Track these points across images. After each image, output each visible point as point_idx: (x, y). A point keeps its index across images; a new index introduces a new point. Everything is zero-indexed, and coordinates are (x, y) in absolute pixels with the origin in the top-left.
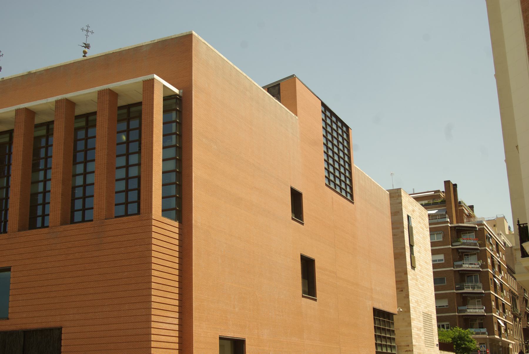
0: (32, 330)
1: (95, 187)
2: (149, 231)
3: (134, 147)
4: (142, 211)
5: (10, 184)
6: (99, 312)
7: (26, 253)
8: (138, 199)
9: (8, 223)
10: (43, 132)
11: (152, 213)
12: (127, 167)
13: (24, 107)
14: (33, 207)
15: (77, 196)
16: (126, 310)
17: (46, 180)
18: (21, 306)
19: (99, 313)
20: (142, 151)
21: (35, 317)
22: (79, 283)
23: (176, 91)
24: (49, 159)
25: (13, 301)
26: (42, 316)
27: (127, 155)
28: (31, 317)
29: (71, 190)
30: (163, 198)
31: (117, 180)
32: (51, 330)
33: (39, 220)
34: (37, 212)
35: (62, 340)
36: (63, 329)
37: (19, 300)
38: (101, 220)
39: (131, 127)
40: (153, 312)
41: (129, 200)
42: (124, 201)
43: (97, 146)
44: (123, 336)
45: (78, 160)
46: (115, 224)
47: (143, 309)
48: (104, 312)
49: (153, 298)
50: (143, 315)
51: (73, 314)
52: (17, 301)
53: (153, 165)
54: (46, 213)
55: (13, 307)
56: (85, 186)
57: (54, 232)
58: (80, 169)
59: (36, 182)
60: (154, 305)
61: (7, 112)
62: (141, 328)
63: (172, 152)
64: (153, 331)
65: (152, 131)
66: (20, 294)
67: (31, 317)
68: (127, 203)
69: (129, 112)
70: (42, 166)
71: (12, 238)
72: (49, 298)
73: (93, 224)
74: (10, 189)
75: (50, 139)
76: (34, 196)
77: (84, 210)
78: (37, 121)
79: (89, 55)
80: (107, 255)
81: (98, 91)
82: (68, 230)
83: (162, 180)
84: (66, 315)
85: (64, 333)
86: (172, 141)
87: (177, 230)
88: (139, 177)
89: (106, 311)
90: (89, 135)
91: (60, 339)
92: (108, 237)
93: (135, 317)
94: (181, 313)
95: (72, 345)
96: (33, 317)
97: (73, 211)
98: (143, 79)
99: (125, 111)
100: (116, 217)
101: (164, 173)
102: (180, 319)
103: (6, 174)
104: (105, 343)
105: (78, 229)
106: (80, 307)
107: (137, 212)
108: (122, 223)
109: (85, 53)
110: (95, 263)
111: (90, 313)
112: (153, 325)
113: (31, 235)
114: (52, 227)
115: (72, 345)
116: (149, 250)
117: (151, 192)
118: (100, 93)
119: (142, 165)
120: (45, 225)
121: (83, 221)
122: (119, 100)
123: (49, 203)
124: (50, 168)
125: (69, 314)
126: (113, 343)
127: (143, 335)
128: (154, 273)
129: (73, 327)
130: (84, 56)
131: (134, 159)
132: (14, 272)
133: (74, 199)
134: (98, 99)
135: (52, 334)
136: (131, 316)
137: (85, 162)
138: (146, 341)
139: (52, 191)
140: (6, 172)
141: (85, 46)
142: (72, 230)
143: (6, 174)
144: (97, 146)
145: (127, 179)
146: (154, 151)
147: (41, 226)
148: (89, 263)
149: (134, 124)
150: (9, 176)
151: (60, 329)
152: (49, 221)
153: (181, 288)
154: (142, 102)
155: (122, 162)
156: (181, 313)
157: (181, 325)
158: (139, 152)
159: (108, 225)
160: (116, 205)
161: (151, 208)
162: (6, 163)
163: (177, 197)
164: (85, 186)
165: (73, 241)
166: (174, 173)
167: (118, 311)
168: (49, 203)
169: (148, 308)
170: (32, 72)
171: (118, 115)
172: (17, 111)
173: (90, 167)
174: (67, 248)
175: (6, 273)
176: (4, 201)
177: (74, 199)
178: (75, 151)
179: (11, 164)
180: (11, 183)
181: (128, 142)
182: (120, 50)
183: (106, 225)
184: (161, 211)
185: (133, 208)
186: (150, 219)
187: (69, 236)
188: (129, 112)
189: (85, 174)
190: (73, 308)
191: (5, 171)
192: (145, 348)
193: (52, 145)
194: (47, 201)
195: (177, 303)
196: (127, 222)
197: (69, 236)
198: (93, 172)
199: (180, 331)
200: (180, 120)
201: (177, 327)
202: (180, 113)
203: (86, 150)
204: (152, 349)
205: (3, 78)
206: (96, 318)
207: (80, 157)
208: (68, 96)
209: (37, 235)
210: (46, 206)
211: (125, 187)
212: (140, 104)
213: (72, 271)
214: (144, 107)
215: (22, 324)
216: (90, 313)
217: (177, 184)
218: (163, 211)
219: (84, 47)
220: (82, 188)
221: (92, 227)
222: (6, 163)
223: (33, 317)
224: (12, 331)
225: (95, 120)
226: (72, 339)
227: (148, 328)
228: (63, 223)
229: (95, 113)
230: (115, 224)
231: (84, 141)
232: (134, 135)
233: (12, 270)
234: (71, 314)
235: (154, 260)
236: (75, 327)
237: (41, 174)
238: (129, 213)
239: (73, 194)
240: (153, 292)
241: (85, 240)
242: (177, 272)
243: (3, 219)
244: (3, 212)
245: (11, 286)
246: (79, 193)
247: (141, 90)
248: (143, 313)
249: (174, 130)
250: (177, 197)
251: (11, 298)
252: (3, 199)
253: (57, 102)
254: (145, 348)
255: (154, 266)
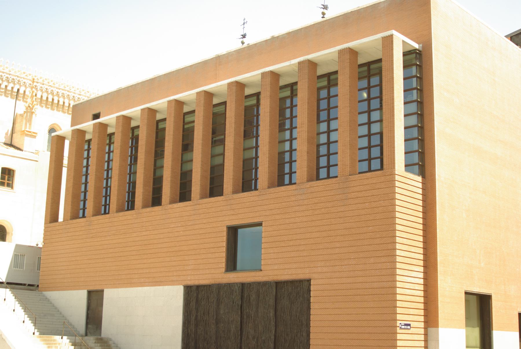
0: (283, 281)
1: (339, 144)
2: (392, 186)
3: (375, 104)
4: (385, 167)
5: (259, 144)
6: (346, 265)
7: (276, 209)
8: (381, 155)
9: (258, 181)
10: (287, 93)
11: (395, 169)
12: (369, 123)
13: (269, 70)
14: (281, 165)
15: (321, 154)
16: (371, 263)
17: (292, 139)
18: (272, 259)
19: (345, 266)
20: (384, 107)
21: (286, 269)
22: (326, 237)
23: (416, 46)
24: (294, 119)
25: (265, 254)
26: (292, 269)
27: (369, 112)
28: (282, 269)
29: (315, 148)
30: (406, 153)
31: (360, 137)
32: (301, 281)
33: (287, 177)
34: (284, 170)
35: (311, 291)
36: (312, 281)
37: (271, 253)
38: (345, 176)
39: (372, 84)
40: (398, 265)
41: (372, 157)
42: (367, 157)
43: (339, 104)
44: (369, 289)
45: (321, 119)
46: (359, 180)
47: (388, 262)
48: (350, 265)
49: (398, 252)
50: (389, 269)
51: (321, 267)
52: (269, 253)
53: (394, 121)
54: (293, 171)
55: (265, 259)
56: (329, 143)
57: (301, 189)
58: (323, 127)
59: (283, 141)
60: (398, 259)
61: (254, 76)
62: (386, 281)
63: (413, 107)
64: (398, 284)
65: (393, 87)
66: (271, 248)
67: (282, 269)
68: (370, 159)
69: (369, 70)
70: (288, 126)
71: (263, 195)
72: (298, 251)
73: (337, 180)
74: (259, 149)
75: (294, 99)
76: (281, 154)
77: (328, 167)
78: (282, 82)
79: (327, 17)
80: (352, 210)
81: (339, 51)
82: (314, 187)
83: (405, 136)
84: (315, 267)
85: (313, 285)
86: (413, 96)
87: (420, 185)
88: (381, 134)
89: (352, 265)
90: (331, 94)
91: (309, 291)
92: (352, 193)
93: (381, 270)
94: (426, 267)
95: (321, 296)
96: (284, 269)
97: (318, 168)
98: (382, 36)
99: (365, 68)
100: (360, 173)
101: (405, 128)
102: (425, 273)
103: (255, 135)
104: (352, 295)
105: (324, 185)
106: (328, 260)
107: (379, 168)
108: (366, 179)
109: (323, 14)
110: (341, 218)
111: (337, 266)
112: (398, 278)
113: (279, 192)
114: (299, 183)
115: (321, 296)
116: (393, 204)
117: (394, 147)
118: (341, 52)
119: (384, 122)
120: (293, 182)
121: (328, 177)
122: (359, 58)
123: (295, 161)
124: (296, 128)
125: (317, 267)
126: (359, 295)
127: (388, 288)
128: (398, 227)
129: (321, 279)
130: (323, 17)
131: (375, 116)
132: (265, 226)
133: (318, 157)
134: (339, 58)
135: (301, 286)
136: (376, 269)
137: (329, 120)
138: (391, 294)
139: (298, 149)
140: (255, 132)
141: (323, 7)
142: (318, 186)
143: (255, 135)
144: (339, 105)
145: (369, 135)
146: (395, 107)
147: (288, 183)
148: (334, 218)
149: (375, 81)
150: (257, 136)
151: (309, 281)
152: (296, 178)
153: (426, 243)
154: (382, 59)
155: (364, 118)
156: (426, 267)
157: (426, 279)
158: (381, 108)
159: (352, 181)
160: (359, 161)
161: (394, 163)
162: (255, 124)
163: (419, 152)
164: (329, 143)
165: (320, 197)
166: (416, 128)
167: (364, 264)
168: (295, 161)
169: (393, 262)
170: (275, 36)
171: (359, 73)
172: (263, 74)
173: (334, 125)
174: (313, 204)
175: (258, 228)
176: (254, 160)
177: (318, 157)
178: (319, 110)
179: (259, 125)
180: (260, 143)
181: (369, 99)
182: (358, 9)
183: (350, 181)
184: (404, 166)
185: (376, 164)
186: (393, 174)
187: (315, 192)
188: (369, 70)
189: (329, 132)
190: (321, 261)
191: (254, 132)
192: (391, 300)
193: (296, 106)
194: (293, 159)
195: (421, 257)
196: (371, 178)
197: (315, 192)
198: (337, 130)
199: (425, 285)
200: (420, 74)
201: (422, 281)
202: (420, 67)
203: (329, 109)
204: (398, 302)
205: (249, 44)
206: (343, 271)
207: (324, 115)
208: (310, 57)
209: (285, 191)
210: (293, 163)
211: (367, 144)
212: (380, 61)
213: (319, 226)
214: (383, 63)
215: (274, 275)
216: (337, 266)
217: (419, 139)
218: (406, 166)
219: (322, 9)
220: (326, 146)
221: (337, 183)
222: (255, 124)
223: (284, 269)
224: (265, 282)
225: (337, 79)
226: (321, 290)
227: (393, 281)
228: (310, 180)
229: (336, 72)
230: (359, 180)
231: (326, 100)
232: (375, 92)
233: (263, 225)
234: (319, 267)
235: (398, 215)
236: (323, 279)
237: (287, 134)
238: (372, 169)
239: (318, 151)
240: (398, 246)
241: (330, 196)
242: (421, 227)
243: (253, 177)
244: (254, 171)
245: (263, 240)
246: (323, 150)
247: (380, 47)
248: (389, 267)
249: (414, 86)
250: (419, 152)
251: (263, 251)
252: (254, 158)
253: (300, 63)
254: (391, 300)
255: (398, 221)
